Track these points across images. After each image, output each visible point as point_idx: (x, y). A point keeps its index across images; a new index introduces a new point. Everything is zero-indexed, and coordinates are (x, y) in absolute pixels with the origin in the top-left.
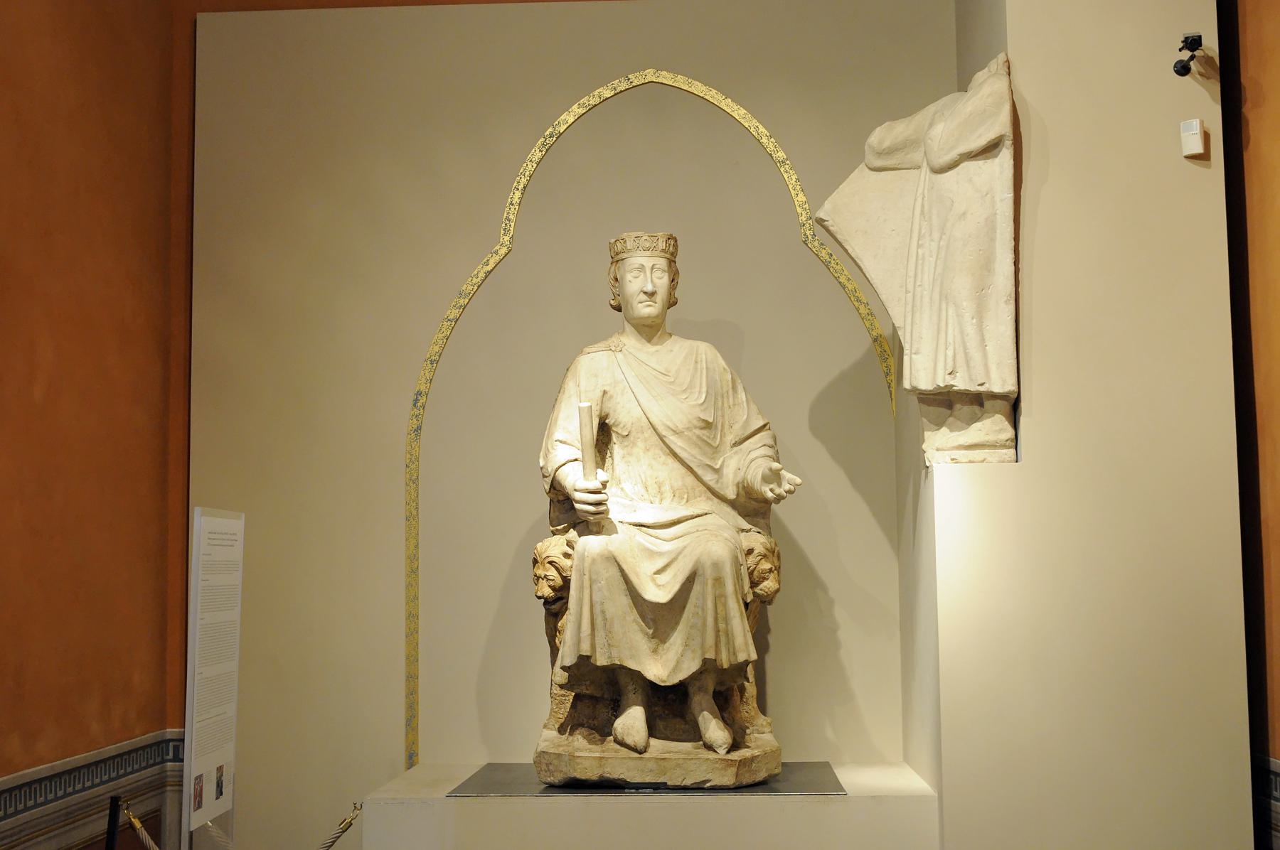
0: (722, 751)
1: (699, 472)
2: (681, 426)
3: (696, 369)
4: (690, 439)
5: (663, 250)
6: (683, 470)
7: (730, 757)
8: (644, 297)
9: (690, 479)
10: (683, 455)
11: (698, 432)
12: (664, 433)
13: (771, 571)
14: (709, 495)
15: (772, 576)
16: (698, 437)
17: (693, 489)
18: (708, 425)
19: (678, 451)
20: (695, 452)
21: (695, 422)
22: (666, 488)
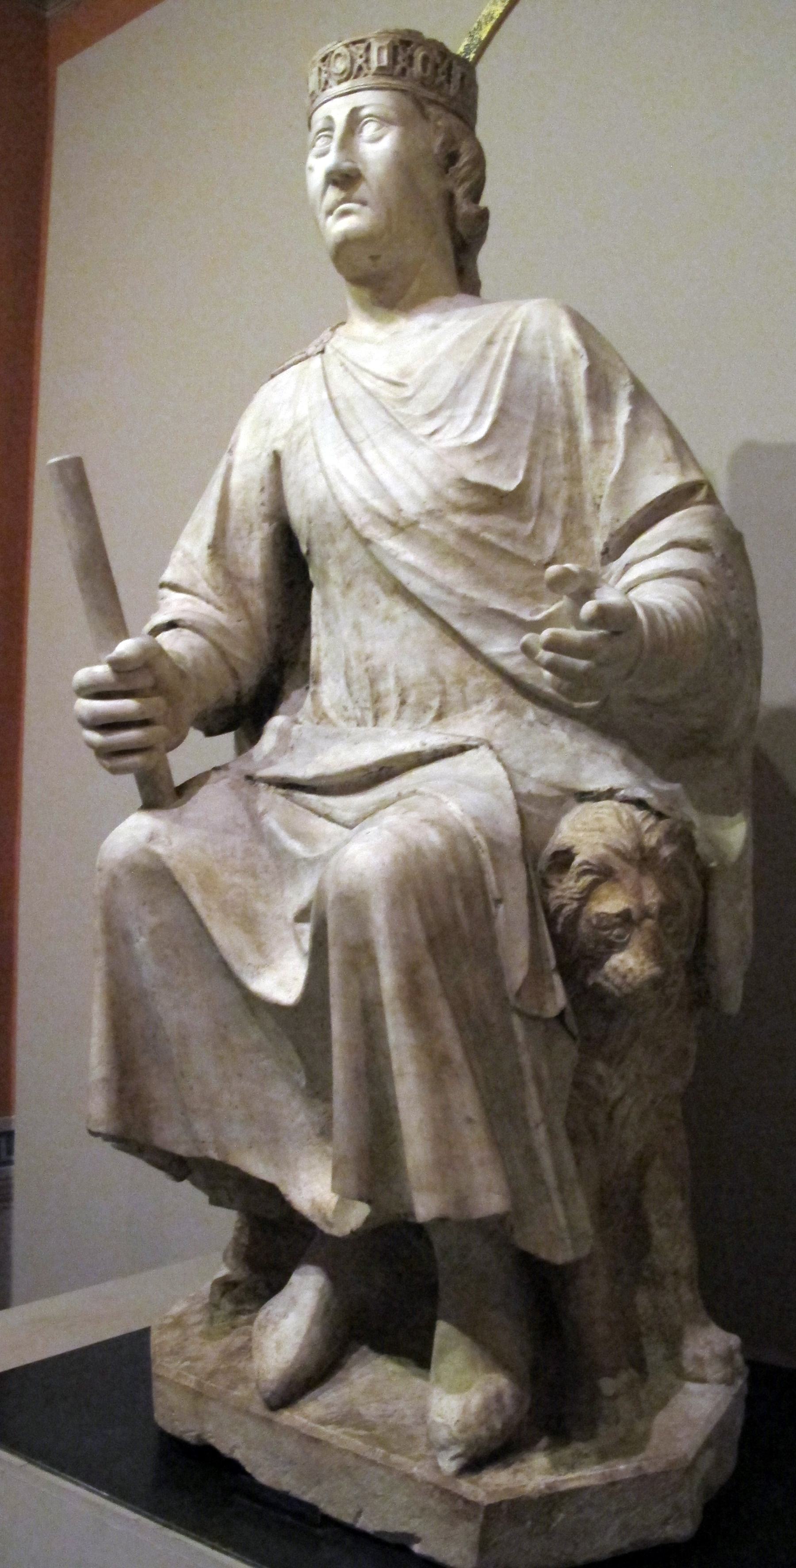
0: (448, 1464)
1: (471, 632)
2: (410, 509)
3: (482, 357)
4: (435, 541)
5: (381, 71)
6: (431, 631)
7: (465, 1487)
8: (333, 194)
9: (450, 658)
10: (418, 586)
11: (460, 520)
12: (370, 532)
13: (625, 919)
14: (512, 697)
15: (638, 938)
16: (465, 534)
17: (461, 681)
18: (491, 500)
19: (404, 576)
20: (453, 576)
21: (453, 494)
22: (388, 685)
